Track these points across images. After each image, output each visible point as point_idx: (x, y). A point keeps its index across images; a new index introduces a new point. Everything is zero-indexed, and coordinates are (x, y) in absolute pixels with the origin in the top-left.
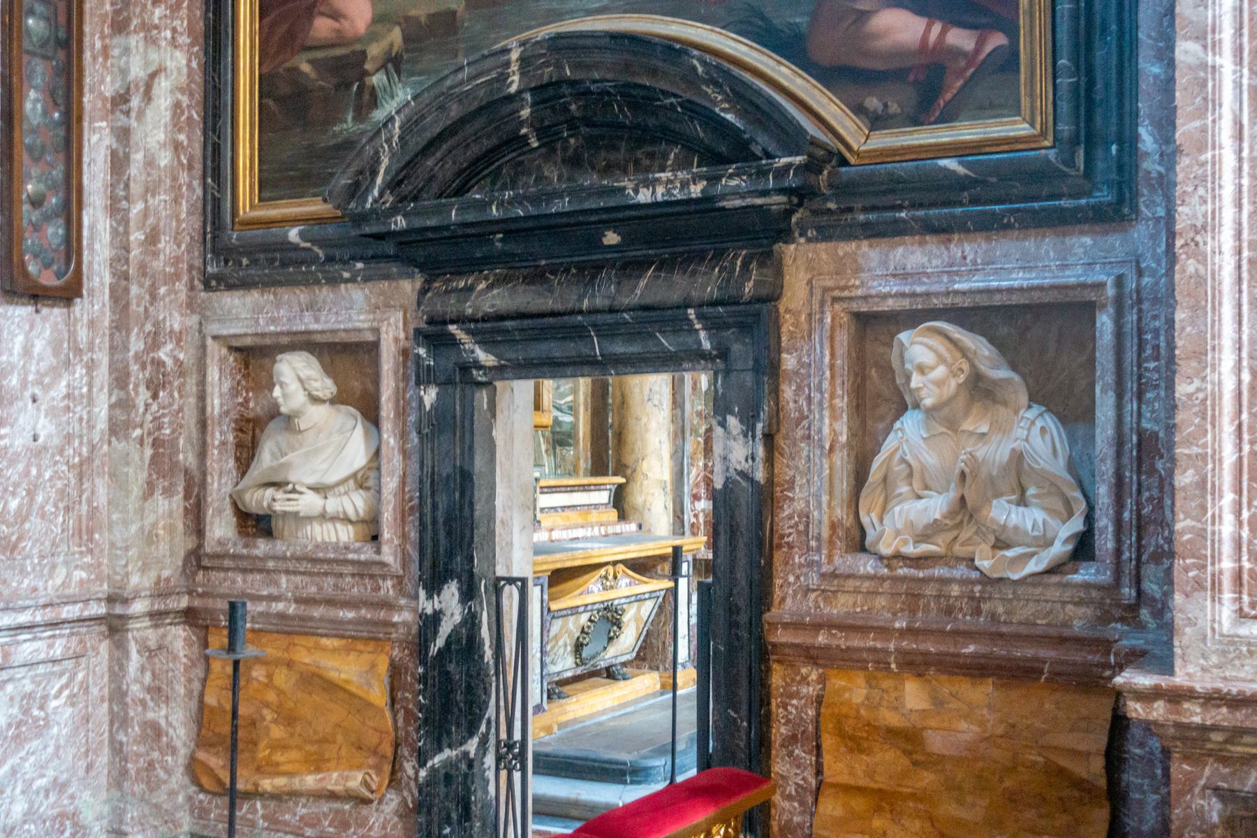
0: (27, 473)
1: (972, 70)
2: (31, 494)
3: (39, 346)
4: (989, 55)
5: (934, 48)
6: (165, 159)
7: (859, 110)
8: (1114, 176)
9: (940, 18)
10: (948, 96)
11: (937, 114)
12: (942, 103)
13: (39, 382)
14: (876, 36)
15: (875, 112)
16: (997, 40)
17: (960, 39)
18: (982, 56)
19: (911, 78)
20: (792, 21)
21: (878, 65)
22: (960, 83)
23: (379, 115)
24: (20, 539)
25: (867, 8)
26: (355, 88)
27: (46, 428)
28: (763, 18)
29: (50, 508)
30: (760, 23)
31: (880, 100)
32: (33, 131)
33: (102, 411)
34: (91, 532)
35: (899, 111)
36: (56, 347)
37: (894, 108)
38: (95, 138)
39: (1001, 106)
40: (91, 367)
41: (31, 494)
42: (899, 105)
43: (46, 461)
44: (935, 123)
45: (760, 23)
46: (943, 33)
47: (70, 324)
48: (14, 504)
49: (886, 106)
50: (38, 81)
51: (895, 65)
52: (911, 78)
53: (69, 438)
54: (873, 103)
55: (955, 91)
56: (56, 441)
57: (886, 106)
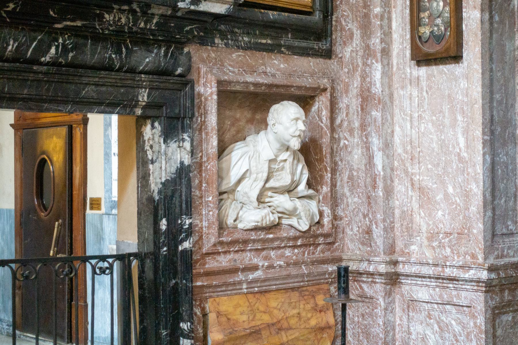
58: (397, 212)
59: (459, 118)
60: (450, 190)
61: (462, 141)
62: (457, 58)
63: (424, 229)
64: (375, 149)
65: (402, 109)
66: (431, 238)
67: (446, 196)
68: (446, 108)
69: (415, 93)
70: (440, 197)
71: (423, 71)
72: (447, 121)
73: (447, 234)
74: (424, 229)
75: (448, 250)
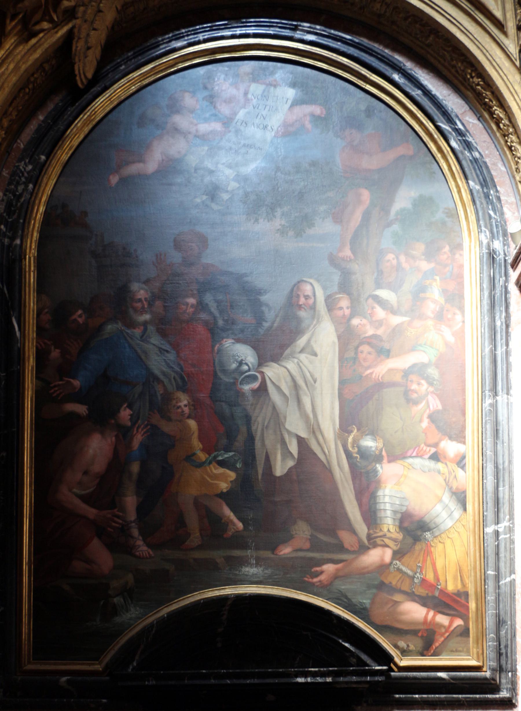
1: (447, 634)
4: (455, 628)
5: (430, 622)
7: (396, 646)
8: (509, 686)
9: (433, 609)
10: (437, 644)
11: (432, 652)
12: (434, 647)
14: (401, 613)
15: (403, 648)
16: (459, 622)
17: (442, 619)
18: (452, 628)
19: (420, 634)
20: (361, 601)
21: (405, 628)
22: (443, 639)
23: (118, 619)
25: (398, 600)
26: (102, 603)
28: (346, 597)
30: (345, 600)
31: (405, 643)
35: (414, 649)
37: (412, 647)
39: (460, 651)
42: (415, 646)
44: (431, 656)
45: (345, 600)
46: (434, 616)
49: (408, 646)
51: (413, 628)
52: (420, 634)
54: (402, 644)
55: (440, 643)
57: (408, 646)
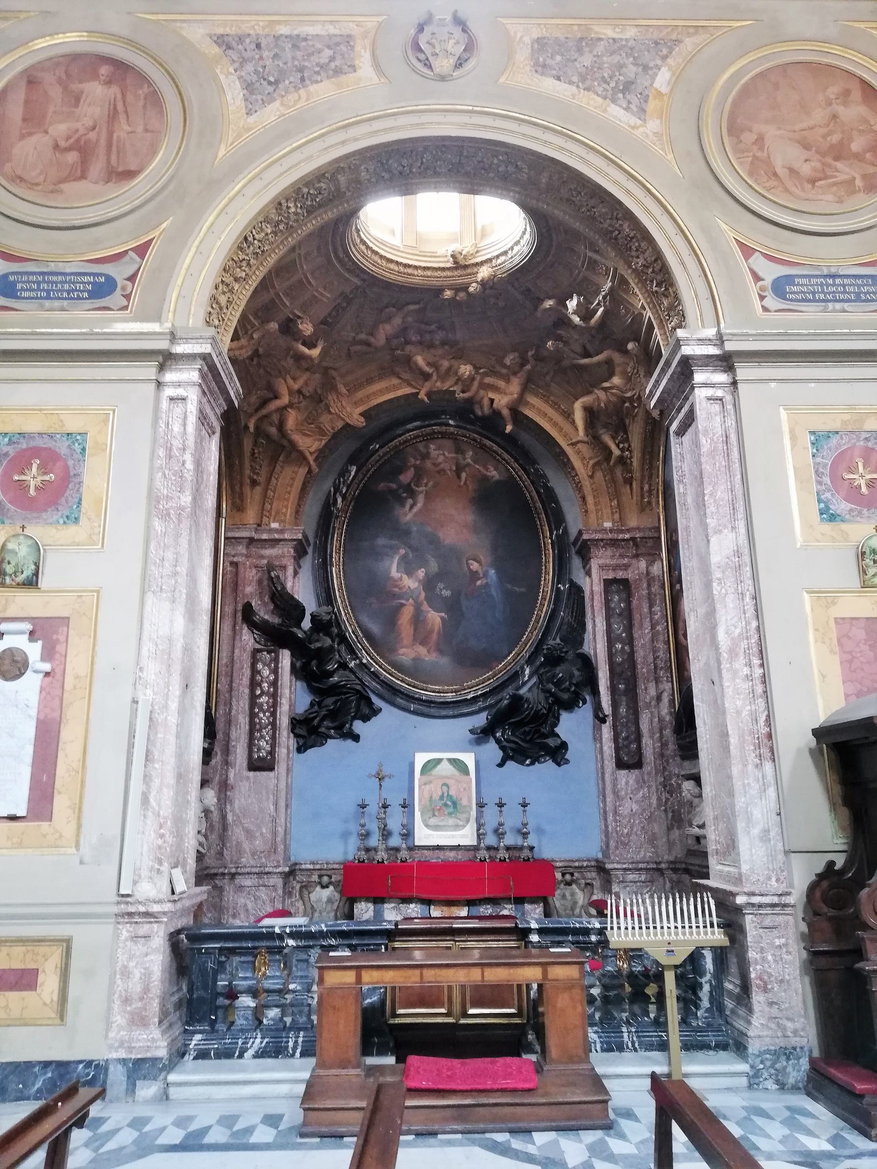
0: (630, 821)
2: (632, 828)
3: (631, 782)
6: (668, 718)
13: (632, 793)
24: (629, 841)
27: (635, 807)
29: (639, 832)
32: (623, 718)
33: (654, 801)
34: (653, 841)
36: (637, 782)
38: (644, 716)
40: (649, 787)
41: (632, 828)
43: (636, 817)
47: (642, 775)
48: (626, 831)
50: (624, 703)
53: (644, 810)
56: (639, 811)
58: (234, 843)
59: (271, 797)
60: (264, 831)
61: (272, 807)
62: (272, 769)
63: (248, 850)
64: (228, 811)
65: (240, 792)
66: (253, 854)
67: (262, 834)
68: (264, 792)
69: (247, 784)
70: (258, 834)
71: (251, 774)
72: (264, 798)
73: (261, 852)
74: (248, 850)
75: (264, 860)
